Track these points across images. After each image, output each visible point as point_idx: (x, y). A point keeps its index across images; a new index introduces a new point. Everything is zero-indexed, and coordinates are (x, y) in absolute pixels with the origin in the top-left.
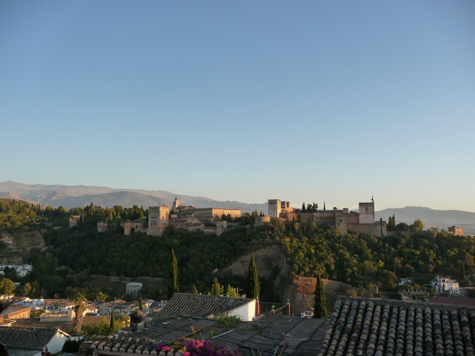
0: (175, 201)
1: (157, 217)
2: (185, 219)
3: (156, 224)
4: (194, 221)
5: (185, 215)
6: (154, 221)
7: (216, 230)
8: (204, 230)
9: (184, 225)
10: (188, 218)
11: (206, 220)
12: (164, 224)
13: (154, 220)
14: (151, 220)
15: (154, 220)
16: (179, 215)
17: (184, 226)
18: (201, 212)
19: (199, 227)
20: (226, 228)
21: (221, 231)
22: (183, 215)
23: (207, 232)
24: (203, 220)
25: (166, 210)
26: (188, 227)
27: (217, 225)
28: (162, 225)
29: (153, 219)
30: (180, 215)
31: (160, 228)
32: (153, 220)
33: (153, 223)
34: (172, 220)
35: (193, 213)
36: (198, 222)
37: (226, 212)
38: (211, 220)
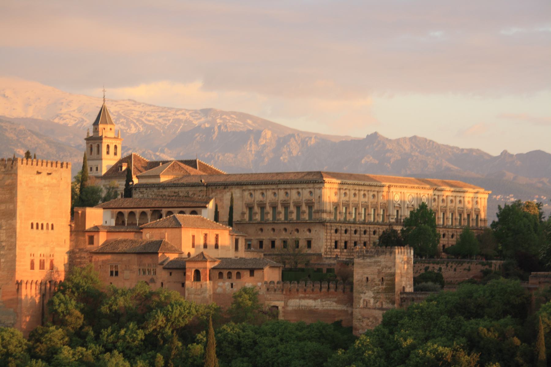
0: (96, 130)
2: (167, 235)
5: (164, 211)
7: (350, 301)
8: (280, 304)
9: (159, 269)
11: (285, 242)
12: (42, 266)
17: (162, 275)
18: (258, 196)
19: (248, 282)
20: (410, 289)
21: (381, 309)
24: (266, 244)
25: (54, 181)
26: (183, 285)
27: (358, 274)
28: (32, 267)
30: (132, 214)
31: (19, 284)
34: (91, 241)
35: (210, 199)
36: (242, 253)
38: (313, 245)
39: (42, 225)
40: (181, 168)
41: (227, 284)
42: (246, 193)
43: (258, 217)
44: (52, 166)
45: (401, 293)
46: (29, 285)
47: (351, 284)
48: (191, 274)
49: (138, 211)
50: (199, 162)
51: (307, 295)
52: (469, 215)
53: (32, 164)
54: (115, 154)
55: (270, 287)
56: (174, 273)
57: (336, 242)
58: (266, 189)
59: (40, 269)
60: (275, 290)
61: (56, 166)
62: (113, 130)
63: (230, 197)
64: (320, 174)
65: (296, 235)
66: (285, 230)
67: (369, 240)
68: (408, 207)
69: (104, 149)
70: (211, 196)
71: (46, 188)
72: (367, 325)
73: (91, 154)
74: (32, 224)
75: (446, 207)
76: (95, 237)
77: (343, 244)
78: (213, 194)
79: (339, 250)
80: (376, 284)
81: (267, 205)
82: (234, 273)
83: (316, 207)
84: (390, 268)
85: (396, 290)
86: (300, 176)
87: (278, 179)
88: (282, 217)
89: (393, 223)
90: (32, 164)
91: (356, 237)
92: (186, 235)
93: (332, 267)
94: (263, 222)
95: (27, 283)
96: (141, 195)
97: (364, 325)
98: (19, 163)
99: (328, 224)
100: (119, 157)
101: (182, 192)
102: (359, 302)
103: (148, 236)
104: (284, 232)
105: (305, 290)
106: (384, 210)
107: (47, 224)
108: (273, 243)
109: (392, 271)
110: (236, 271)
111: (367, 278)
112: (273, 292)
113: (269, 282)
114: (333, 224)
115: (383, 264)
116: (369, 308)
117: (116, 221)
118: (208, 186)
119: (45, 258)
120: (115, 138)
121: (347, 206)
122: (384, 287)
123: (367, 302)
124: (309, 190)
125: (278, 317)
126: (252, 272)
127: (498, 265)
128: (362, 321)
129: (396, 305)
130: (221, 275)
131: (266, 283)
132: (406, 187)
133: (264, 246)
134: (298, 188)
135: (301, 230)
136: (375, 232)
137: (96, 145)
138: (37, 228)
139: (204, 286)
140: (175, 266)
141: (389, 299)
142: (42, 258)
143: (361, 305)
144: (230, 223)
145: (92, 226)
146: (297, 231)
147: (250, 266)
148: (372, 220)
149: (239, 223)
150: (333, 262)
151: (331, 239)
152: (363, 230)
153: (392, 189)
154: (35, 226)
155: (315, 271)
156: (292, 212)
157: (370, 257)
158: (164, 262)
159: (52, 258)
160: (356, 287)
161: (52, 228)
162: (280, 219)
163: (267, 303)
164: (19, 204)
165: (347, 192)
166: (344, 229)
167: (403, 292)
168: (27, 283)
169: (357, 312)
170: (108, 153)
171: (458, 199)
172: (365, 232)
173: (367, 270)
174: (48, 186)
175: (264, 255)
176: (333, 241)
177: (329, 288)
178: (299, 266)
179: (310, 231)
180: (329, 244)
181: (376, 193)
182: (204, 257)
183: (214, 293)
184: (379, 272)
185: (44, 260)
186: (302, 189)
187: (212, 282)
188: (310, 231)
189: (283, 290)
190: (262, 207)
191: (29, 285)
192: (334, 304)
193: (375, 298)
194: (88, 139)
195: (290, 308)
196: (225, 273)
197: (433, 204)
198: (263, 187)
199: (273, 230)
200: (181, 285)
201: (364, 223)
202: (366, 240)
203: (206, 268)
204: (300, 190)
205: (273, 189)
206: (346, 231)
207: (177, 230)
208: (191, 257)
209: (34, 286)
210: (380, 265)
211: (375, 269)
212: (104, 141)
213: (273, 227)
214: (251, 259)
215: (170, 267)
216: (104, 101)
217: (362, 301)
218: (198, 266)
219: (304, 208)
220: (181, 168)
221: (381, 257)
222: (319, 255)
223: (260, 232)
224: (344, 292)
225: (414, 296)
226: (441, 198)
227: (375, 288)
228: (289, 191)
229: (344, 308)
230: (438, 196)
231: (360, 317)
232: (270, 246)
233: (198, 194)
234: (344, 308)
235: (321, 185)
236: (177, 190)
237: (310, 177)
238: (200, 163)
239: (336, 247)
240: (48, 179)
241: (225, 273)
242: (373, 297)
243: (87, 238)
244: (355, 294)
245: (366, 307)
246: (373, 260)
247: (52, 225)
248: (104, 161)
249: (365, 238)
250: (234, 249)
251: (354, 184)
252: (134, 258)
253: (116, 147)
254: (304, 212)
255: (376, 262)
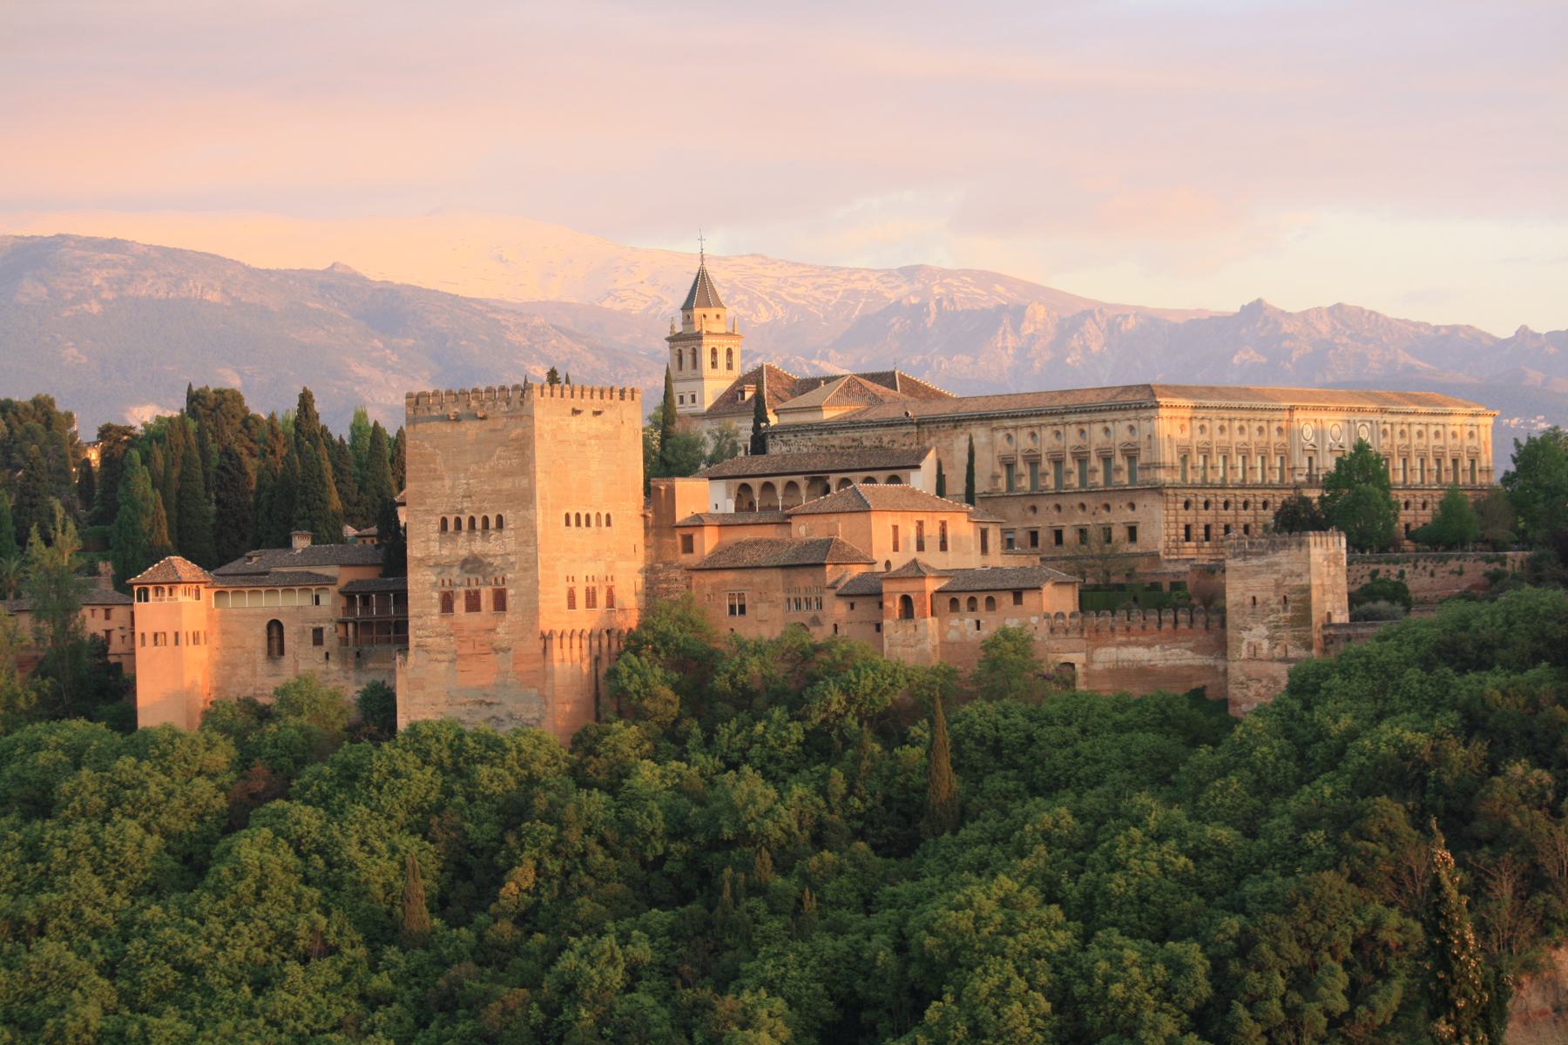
0: (688, 320)
1: (508, 515)
2: (843, 528)
3: (500, 602)
4: (943, 547)
5: (833, 480)
6: (473, 564)
7: (1221, 647)
8: (1078, 659)
9: (828, 597)
10: (875, 518)
11: (1083, 532)
12: (591, 601)
13: (478, 546)
14: (435, 548)
15: (478, 546)
16: (756, 484)
18: (1023, 441)
19: (1009, 617)
20: (1341, 617)
21: (1285, 660)
22: (802, 481)
23: (1120, 673)
24: (1045, 536)
25: (609, 427)
26: (879, 627)
28: (572, 604)
29: (464, 547)
30: (768, 487)
31: (546, 638)
32: (464, 553)
33: (462, 590)
34: (688, 546)
36: (997, 558)
37: (1320, 433)
38: (1140, 534)
39: (588, 516)
40: (863, 392)
41: (969, 621)
42: (1000, 435)
43: (1025, 483)
44: (602, 397)
45: (1324, 627)
46: (566, 641)
47: (1222, 611)
48: (893, 605)
49: (779, 483)
50: (900, 375)
51: (1133, 639)
52: (1455, 461)
53: (562, 396)
54: (730, 367)
55: (1056, 625)
56: (859, 603)
57: (1187, 528)
58: (1040, 426)
59: (588, 607)
60: (1067, 631)
61: (611, 398)
62: (722, 319)
63: (965, 445)
64: (1148, 388)
65: (1105, 518)
66: (1083, 506)
67: (1255, 522)
68: (1331, 451)
69: (706, 358)
70: (927, 444)
71: (593, 442)
72: (1258, 694)
73: (681, 368)
74: (567, 516)
75: (1407, 447)
76: (696, 537)
77: (1202, 531)
78: (933, 439)
79: (1193, 544)
80: (1272, 610)
81: (1044, 456)
82: (981, 599)
83: (1143, 458)
84: (1299, 575)
85: (1314, 619)
86: (1108, 395)
87: (1064, 402)
88: (1074, 480)
89: (1303, 483)
90: (562, 396)
91: (1228, 516)
92: (881, 527)
93: (1182, 579)
94: (1036, 493)
95: (561, 637)
96: (784, 449)
97: (1251, 694)
98: (536, 393)
99: (1170, 492)
100: (737, 372)
101: (869, 438)
102: (1238, 649)
103: (802, 530)
104: (1080, 512)
105: (1128, 629)
106: (1282, 458)
107: (598, 514)
108: (1058, 535)
109: (1304, 582)
110: (985, 596)
111: (1254, 598)
112: (1062, 635)
113: (1053, 615)
114: (1178, 492)
115: (1285, 568)
116: (1261, 660)
117: (736, 502)
118: (920, 423)
119: (596, 584)
120: (727, 334)
121: (1206, 453)
122: (1289, 614)
123: (1255, 648)
124: (1128, 423)
125: (1074, 685)
126: (1018, 595)
127: (1518, 560)
128: (1247, 687)
129: (1314, 652)
130: (954, 603)
131: (1047, 616)
132: (1326, 409)
133: (1040, 541)
134: (1104, 421)
135: (1115, 505)
136: (1265, 505)
137: (690, 350)
138: (578, 524)
139: (921, 629)
140: (860, 591)
141: (1299, 638)
142: (591, 584)
143: (1244, 654)
144: (970, 497)
145: (689, 514)
146: (1107, 507)
147: (1014, 584)
148: (1259, 478)
149: (988, 497)
150: (1182, 568)
151: (1176, 522)
152: (1242, 500)
153: (1298, 415)
154: (573, 520)
155: (1147, 589)
156: (1094, 471)
157: (1258, 554)
158: (837, 582)
159: (610, 583)
160: (1233, 618)
161: (608, 524)
162: (1071, 486)
163: (1051, 657)
164: (539, 476)
165: (1206, 423)
166: (1202, 500)
167: (1328, 624)
168: (561, 637)
169: (1236, 669)
170: (714, 365)
171: (1432, 429)
172: (1246, 505)
173: (1251, 582)
174: (597, 437)
175: (1041, 560)
176: (1182, 525)
177: (1176, 622)
178: (1114, 580)
179: (1132, 506)
180: (1173, 532)
181: (1264, 424)
182: (919, 570)
183: (942, 642)
184: (1278, 586)
185: (594, 588)
186: (1113, 421)
187: (936, 619)
188: (1132, 506)
189: (1082, 630)
190: (1033, 461)
191: (566, 641)
192: (1189, 653)
193: (1270, 638)
194: (674, 339)
195: (1098, 667)
196: (963, 600)
197: (1383, 441)
198: (1034, 421)
199: (1058, 508)
200: (873, 628)
201: (1242, 486)
202: (1249, 520)
203: (924, 591)
204: (1109, 425)
205: (1055, 424)
206: (1207, 505)
207: (861, 517)
208: (893, 568)
209: (576, 642)
210: (1277, 572)
211: (1270, 579)
212: (705, 340)
213: (1058, 502)
214: (1014, 570)
215: (851, 592)
216: (702, 259)
217: (1244, 646)
218: (908, 587)
219: (1119, 461)
220: (863, 392)
221: (1281, 553)
222: (1154, 556)
223: (1030, 514)
224: (1207, 628)
225: (1350, 632)
226: (1398, 429)
227: (1271, 618)
228: (1086, 428)
229: (1210, 661)
230: (1392, 424)
231: (1242, 678)
232: (1053, 540)
233: (901, 440)
234: (1210, 661)
235: (1152, 413)
236: (857, 435)
237: (1129, 398)
238: (900, 375)
239: (1188, 538)
240: (594, 424)
241: (963, 600)
242: (1267, 637)
243: (679, 539)
244: (1230, 633)
245: (1254, 657)
246: (1264, 561)
247: (608, 516)
248: (706, 383)
249: (1246, 516)
250: (979, 551)
251: (1220, 408)
252: (777, 577)
253: (729, 352)
254: (1119, 469)
255: (1269, 565)
